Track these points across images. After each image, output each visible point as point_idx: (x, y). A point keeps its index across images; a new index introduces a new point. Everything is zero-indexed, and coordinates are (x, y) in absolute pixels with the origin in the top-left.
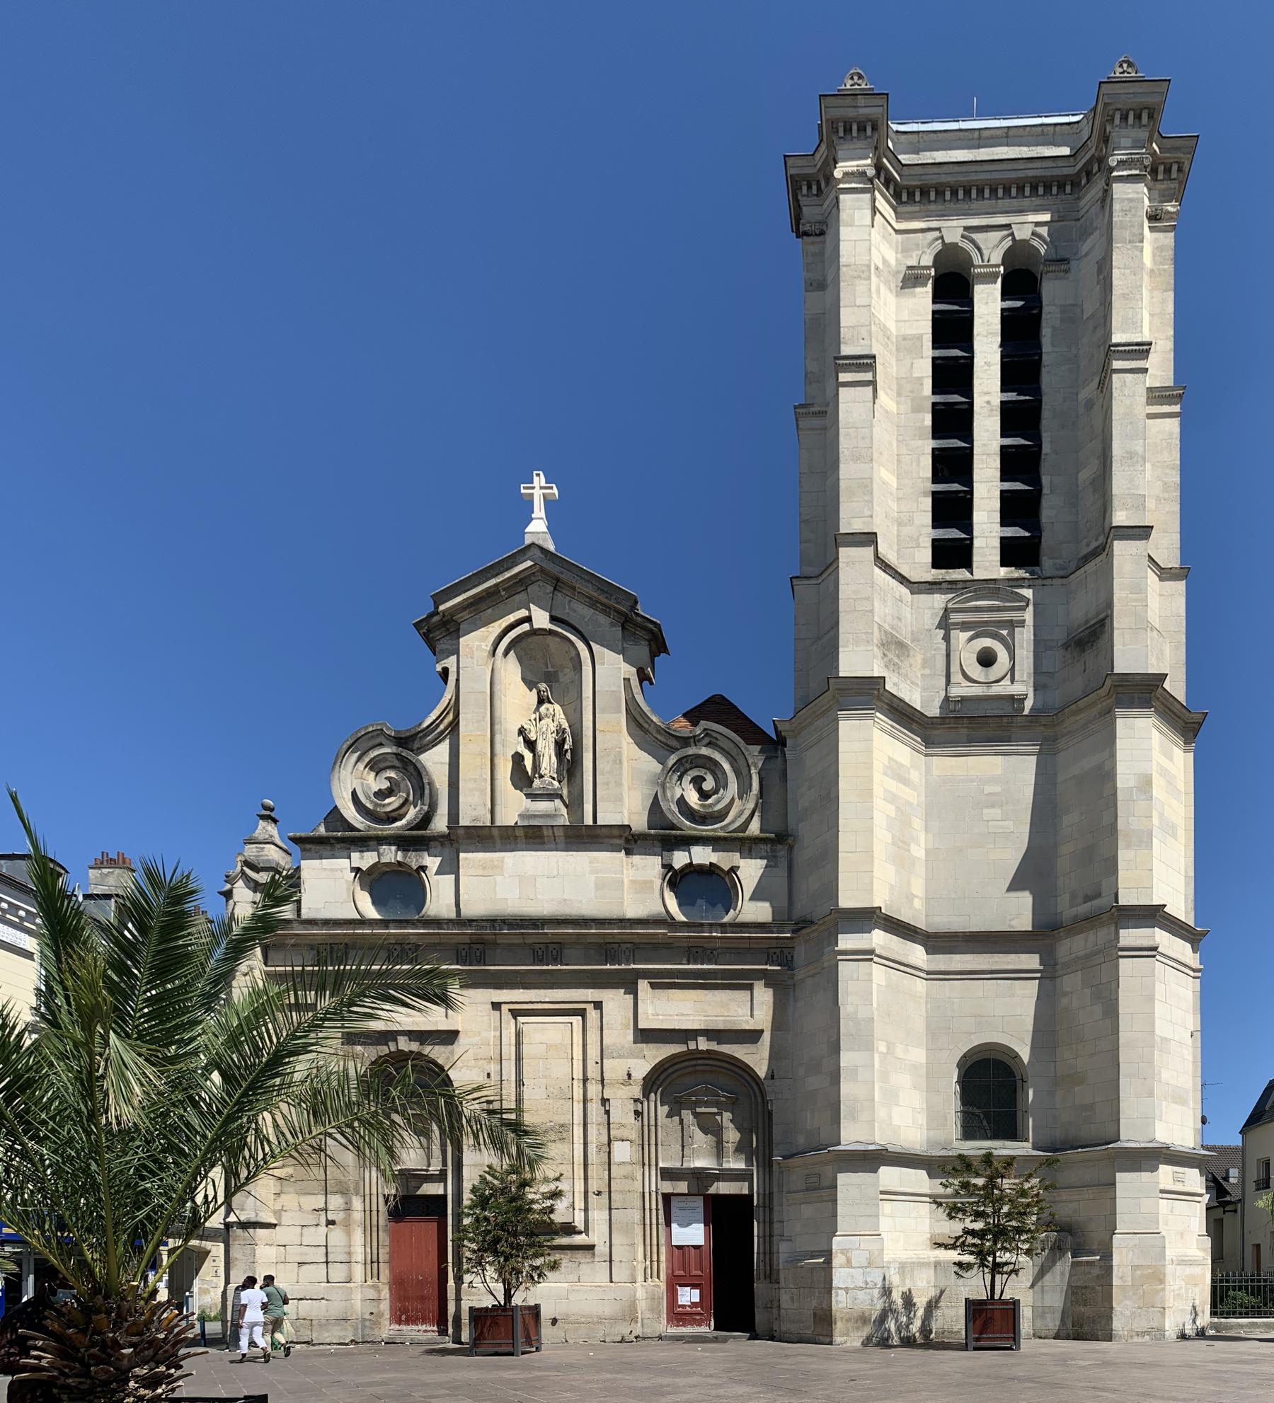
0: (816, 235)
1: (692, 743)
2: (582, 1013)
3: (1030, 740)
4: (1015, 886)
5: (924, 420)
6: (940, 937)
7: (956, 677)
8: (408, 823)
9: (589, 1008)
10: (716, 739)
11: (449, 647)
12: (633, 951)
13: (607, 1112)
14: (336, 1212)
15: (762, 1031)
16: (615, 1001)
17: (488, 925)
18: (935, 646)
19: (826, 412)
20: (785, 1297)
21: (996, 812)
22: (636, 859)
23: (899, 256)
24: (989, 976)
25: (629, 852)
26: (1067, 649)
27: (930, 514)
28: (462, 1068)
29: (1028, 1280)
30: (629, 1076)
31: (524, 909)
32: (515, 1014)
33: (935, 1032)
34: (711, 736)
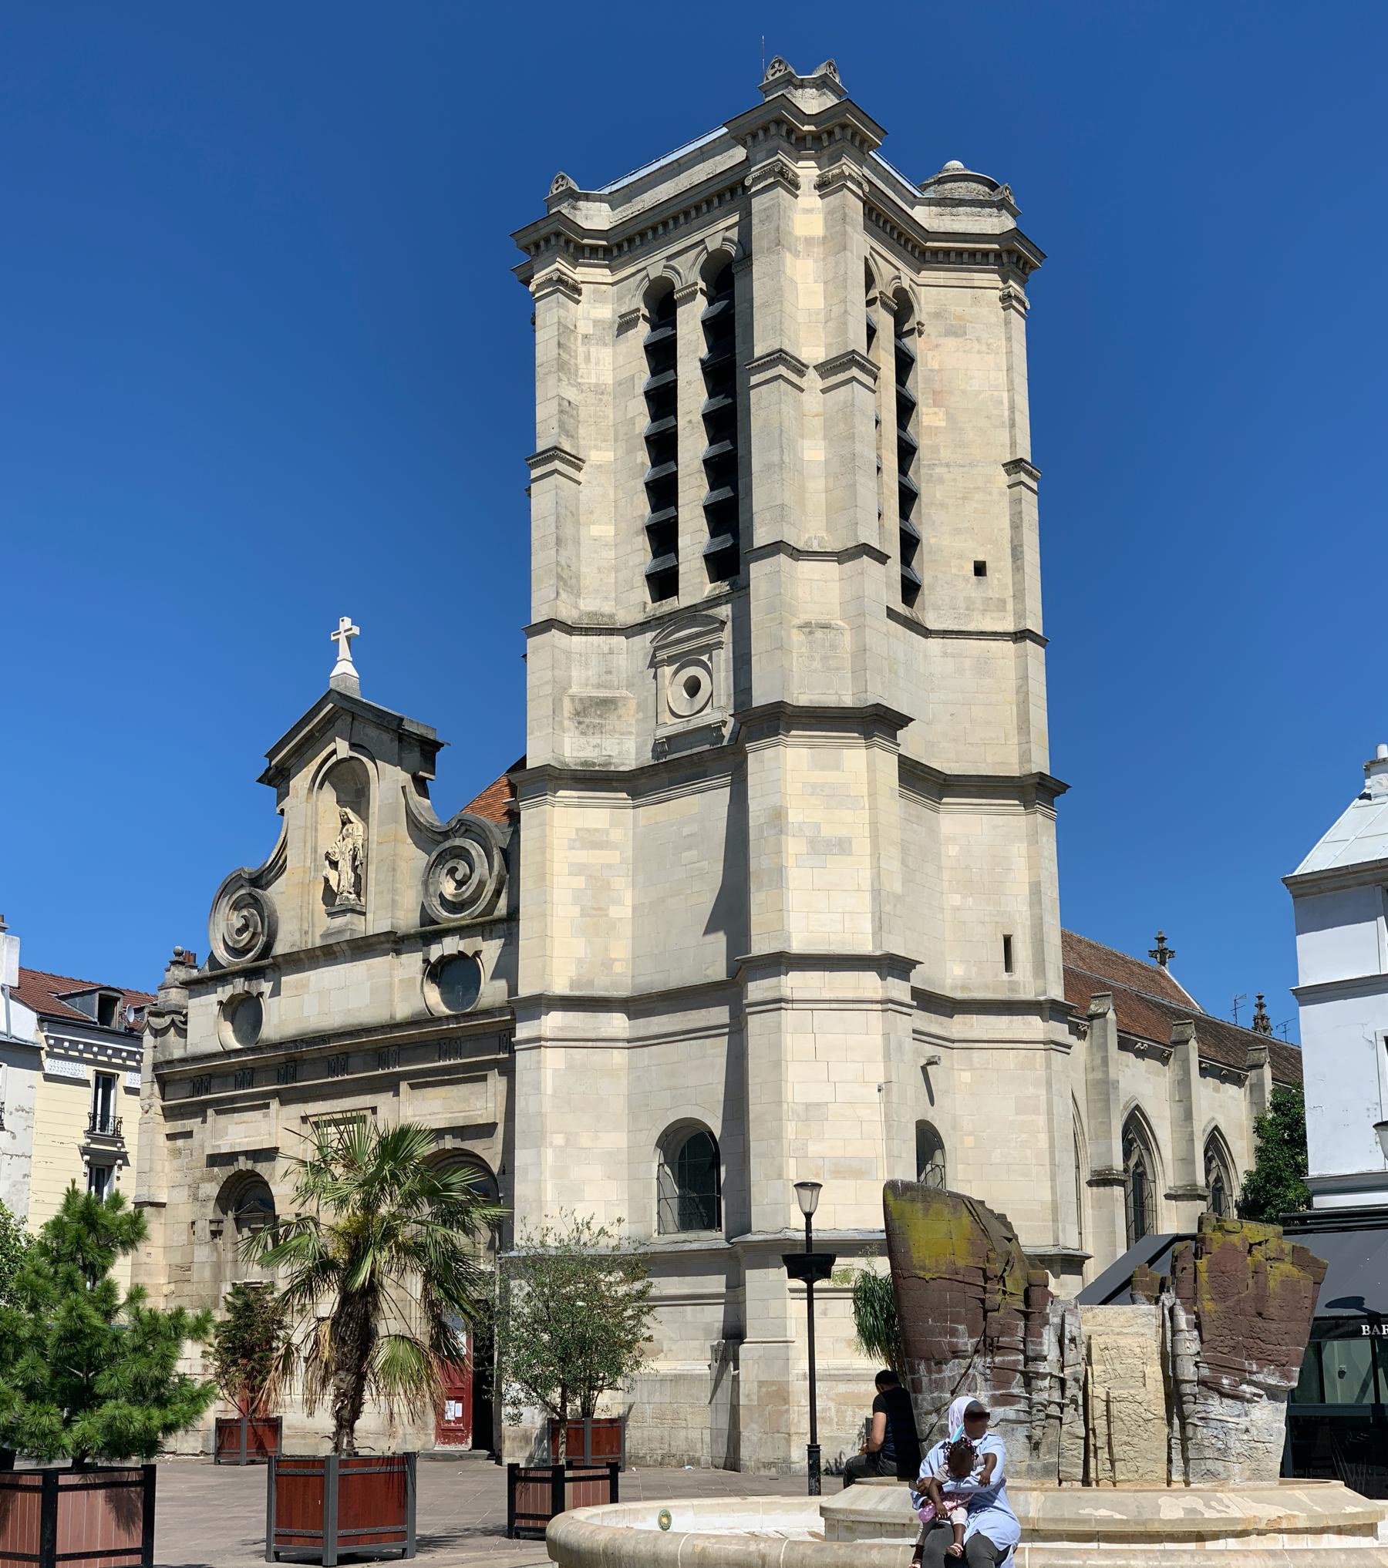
1: (452, 836)
3: (722, 771)
4: (710, 929)
6: (642, 999)
15: (494, 1125)
17: (291, 1045)
22: (404, 957)
24: (682, 1037)
25: (398, 952)
29: (706, 1397)
31: (323, 1024)
33: (637, 1108)
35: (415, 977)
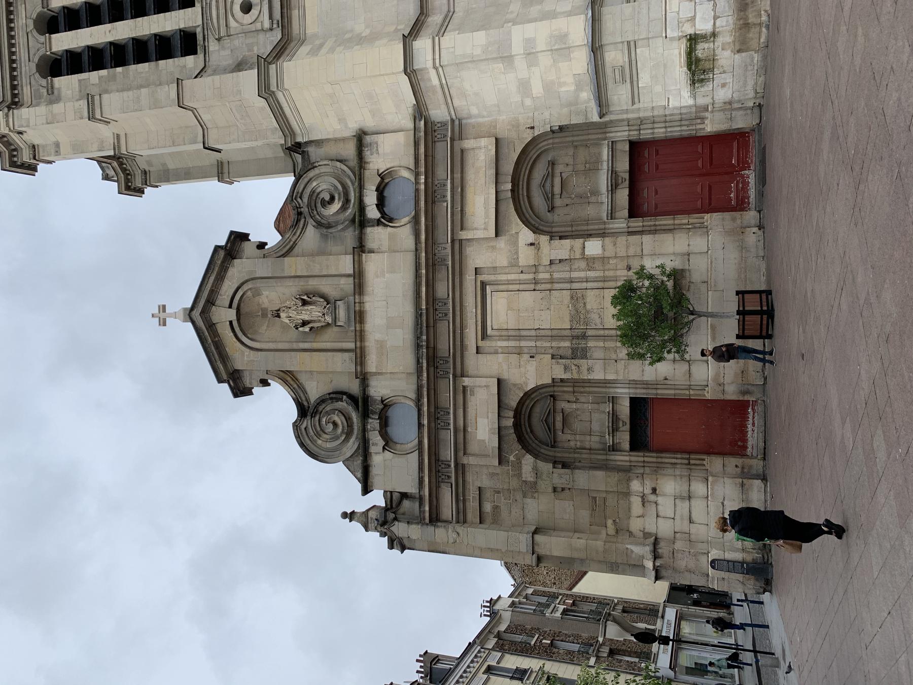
0: (35, 151)
2: (484, 285)
7: (258, 26)
8: (355, 409)
9: (481, 278)
10: (298, 193)
12: (439, 244)
13: (560, 261)
14: (645, 485)
16: (477, 257)
18: (241, 45)
19: (117, 134)
20: (722, 95)
23: (43, 100)
27: (168, 60)
28: (526, 378)
30: (532, 244)
32: (484, 336)
34: (296, 196)
35: (389, 234)
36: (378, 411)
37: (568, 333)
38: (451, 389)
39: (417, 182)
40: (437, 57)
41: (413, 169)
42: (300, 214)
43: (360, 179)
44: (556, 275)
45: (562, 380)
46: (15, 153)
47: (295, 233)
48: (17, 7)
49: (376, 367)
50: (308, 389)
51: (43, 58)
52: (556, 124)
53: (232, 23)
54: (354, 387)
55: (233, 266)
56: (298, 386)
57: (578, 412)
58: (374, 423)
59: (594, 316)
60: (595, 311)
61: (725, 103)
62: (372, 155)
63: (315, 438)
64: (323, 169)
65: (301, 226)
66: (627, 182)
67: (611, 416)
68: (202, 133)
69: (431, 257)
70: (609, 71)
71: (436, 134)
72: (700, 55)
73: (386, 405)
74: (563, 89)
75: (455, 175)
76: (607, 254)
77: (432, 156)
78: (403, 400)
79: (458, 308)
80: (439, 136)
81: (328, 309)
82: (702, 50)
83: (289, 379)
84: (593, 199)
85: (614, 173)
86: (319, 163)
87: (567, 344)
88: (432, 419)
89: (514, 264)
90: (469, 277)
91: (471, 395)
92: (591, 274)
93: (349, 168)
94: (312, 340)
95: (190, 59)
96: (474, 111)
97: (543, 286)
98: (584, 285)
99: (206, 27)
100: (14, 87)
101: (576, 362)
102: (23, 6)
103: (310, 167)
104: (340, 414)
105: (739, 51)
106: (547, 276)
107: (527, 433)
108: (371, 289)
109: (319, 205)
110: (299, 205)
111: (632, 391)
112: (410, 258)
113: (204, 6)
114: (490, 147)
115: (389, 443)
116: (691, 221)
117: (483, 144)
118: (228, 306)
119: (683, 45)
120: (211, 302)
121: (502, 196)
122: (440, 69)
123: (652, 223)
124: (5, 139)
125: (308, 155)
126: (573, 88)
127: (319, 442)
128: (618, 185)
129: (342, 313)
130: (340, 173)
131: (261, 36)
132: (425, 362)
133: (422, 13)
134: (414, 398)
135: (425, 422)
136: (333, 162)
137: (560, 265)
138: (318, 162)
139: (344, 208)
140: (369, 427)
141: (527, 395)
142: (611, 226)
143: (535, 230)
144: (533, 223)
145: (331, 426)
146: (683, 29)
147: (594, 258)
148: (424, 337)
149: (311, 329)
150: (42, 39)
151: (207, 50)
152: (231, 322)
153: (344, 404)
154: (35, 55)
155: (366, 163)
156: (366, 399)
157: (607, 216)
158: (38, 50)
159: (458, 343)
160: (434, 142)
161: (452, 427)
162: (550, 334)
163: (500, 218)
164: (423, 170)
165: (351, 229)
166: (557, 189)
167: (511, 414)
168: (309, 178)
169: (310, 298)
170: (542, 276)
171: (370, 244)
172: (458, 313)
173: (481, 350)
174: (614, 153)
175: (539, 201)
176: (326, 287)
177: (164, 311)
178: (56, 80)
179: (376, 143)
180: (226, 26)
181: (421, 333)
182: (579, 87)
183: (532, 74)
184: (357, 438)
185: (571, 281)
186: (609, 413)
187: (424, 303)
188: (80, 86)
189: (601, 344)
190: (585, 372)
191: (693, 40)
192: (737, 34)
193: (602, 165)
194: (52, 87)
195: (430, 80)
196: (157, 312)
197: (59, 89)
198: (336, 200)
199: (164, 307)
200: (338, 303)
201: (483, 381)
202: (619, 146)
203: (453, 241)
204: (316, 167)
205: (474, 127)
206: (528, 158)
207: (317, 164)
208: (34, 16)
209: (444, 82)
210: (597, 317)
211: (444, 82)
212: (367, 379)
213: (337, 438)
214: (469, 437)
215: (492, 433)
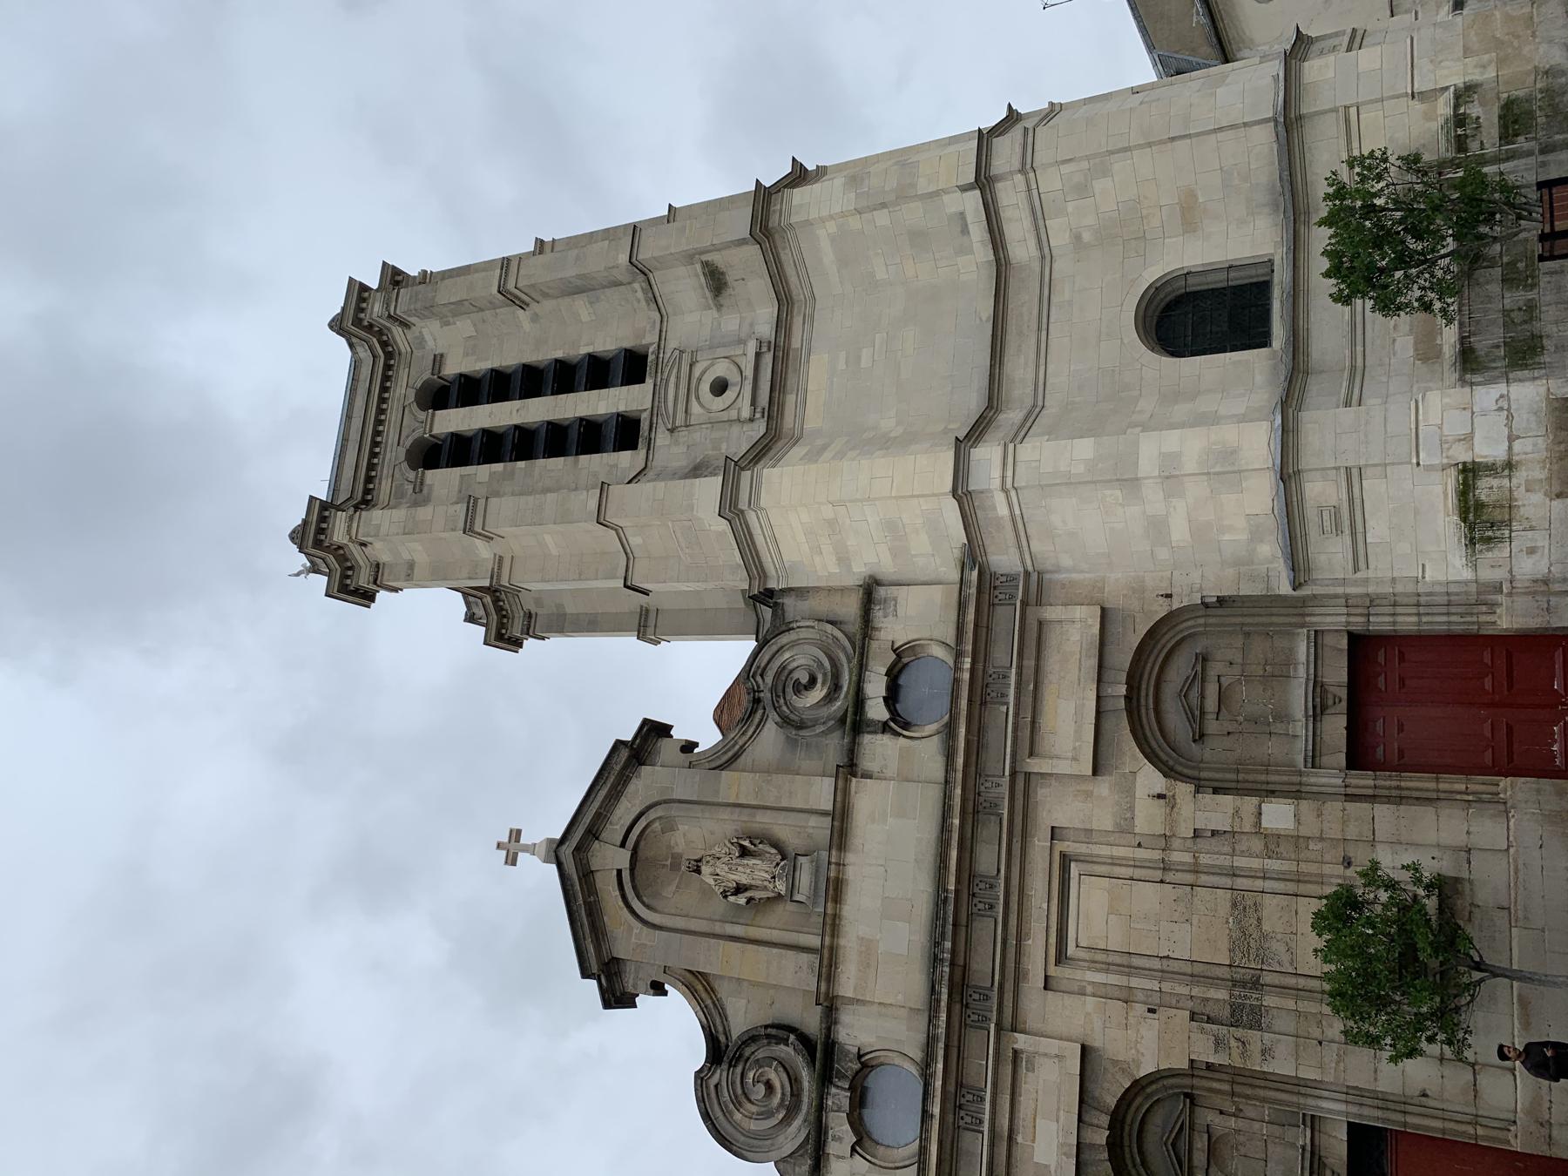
0: (378, 572)
2: (1066, 860)
5: (521, 468)
7: (733, 414)
9: (1060, 846)
10: (758, 667)
11: (632, 977)
13: (1214, 833)
18: (703, 440)
19: (500, 557)
20: (1529, 567)
21: (866, 354)
26: (721, 306)
30: (1160, 796)
32: (1061, 957)
34: (755, 673)
36: (849, 1074)
37: (1224, 972)
38: (991, 1052)
39: (957, 668)
40: (1009, 473)
41: (953, 645)
42: (757, 701)
43: (862, 655)
44: (1205, 859)
45: (1209, 1067)
46: (350, 573)
47: (745, 731)
48: (398, 372)
49: (855, 989)
50: (730, 1012)
51: (418, 443)
52: (1212, 594)
53: (695, 408)
54: (812, 1022)
55: (639, 776)
56: (714, 1003)
57: (1241, 1138)
58: (839, 1097)
59: (1277, 947)
60: (1279, 936)
61: (1535, 581)
62: (885, 617)
63: (731, 1106)
64: (803, 634)
65: (756, 721)
66: (1344, 704)
67: (1308, 1155)
68: (625, 564)
69: (972, 797)
70: (1311, 514)
71: (997, 592)
72: (1483, 497)
73: (866, 1065)
74: (1227, 537)
75: (1025, 663)
76: (1304, 831)
77: (988, 627)
78: (898, 1060)
79: (1014, 898)
80: (1001, 597)
81: (783, 868)
82: (1486, 489)
83: (700, 987)
84: (1279, 728)
85: (1318, 687)
86: (798, 624)
87: (1222, 995)
88: (950, 1106)
89: (1125, 827)
90: (1040, 844)
91: (1027, 1069)
92: (1274, 865)
93: (846, 635)
94: (749, 922)
95: (626, 456)
96: (1066, 561)
97: (1179, 877)
98: (1259, 884)
99: (655, 412)
100: (369, 479)
101: (1239, 1032)
102: (407, 370)
103: (784, 628)
104: (781, 1069)
105: (1558, 496)
106: (1187, 858)
107: (1134, 1166)
108: (861, 841)
109: (789, 690)
110: (758, 687)
111: (1354, 1109)
112: (934, 794)
113: (659, 383)
114: (1090, 621)
115: (863, 1141)
116: (1472, 787)
117: (1078, 616)
118: (619, 843)
119: (1451, 480)
120: (593, 833)
121: (1108, 705)
122: (1013, 493)
123: (1394, 783)
124: (341, 552)
125: (783, 609)
126: (1244, 536)
127: (738, 1116)
128: (1327, 708)
129: (805, 879)
130: (831, 641)
131: (736, 429)
132: (945, 991)
133: (989, 407)
134: (918, 1060)
135: (936, 1110)
136: (821, 623)
137: (1213, 841)
138: (797, 621)
139: (829, 698)
140: (830, 1103)
141: (1138, 1086)
142: (1313, 780)
143: (1168, 772)
144: (1164, 757)
145: (761, 1088)
146: (1451, 453)
147: (1279, 836)
148: (948, 945)
149: (750, 900)
150: (422, 415)
151: (652, 445)
152: (619, 872)
153: (790, 1050)
154: (407, 437)
155: (873, 628)
156: (830, 1046)
157: (1306, 761)
158: (414, 431)
159: (1011, 965)
160: (992, 605)
161: (986, 1128)
162: (1189, 971)
163: (1102, 742)
164: (969, 648)
165: (837, 734)
166: (1211, 704)
167: (1105, 1120)
168: (779, 645)
169: (755, 845)
170: (1177, 857)
171: (867, 762)
172: (1014, 906)
173: (1053, 983)
174: (1320, 651)
175: (1176, 720)
176: (786, 830)
177: (518, 840)
178: (429, 473)
179: (895, 599)
180: (686, 412)
181: (943, 935)
182: (1256, 536)
183: (1172, 509)
184: (805, 1121)
185: (1234, 873)
186: (1303, 1148)
187: (952, 879)
188: (461, 483)
189: (1291, 1004)
190: (1257, 1056)
191: (1470, 473)
192: (1555, 467)
193: (1296, 669)
194: (422, 483)
195: (994, 508)
196: (506, 840)
197: (431, 486)
198: (819, 685)
199: (519, 832)
200: (801, 859)
201: (1052, 1046)
202: (1329, 640)
203: (1013, 774)
204: (793, 629)
205: (1063, 586)
206: (1159, 646)
207: (795, 626)
208: (418, 385)
209: (1017, 512)
210: (1283, 949)
211: (1017, 512)
212: (837, 1009)
213: (769, 1114)
214: (1018, 1153)
215: (1065, 1154)
